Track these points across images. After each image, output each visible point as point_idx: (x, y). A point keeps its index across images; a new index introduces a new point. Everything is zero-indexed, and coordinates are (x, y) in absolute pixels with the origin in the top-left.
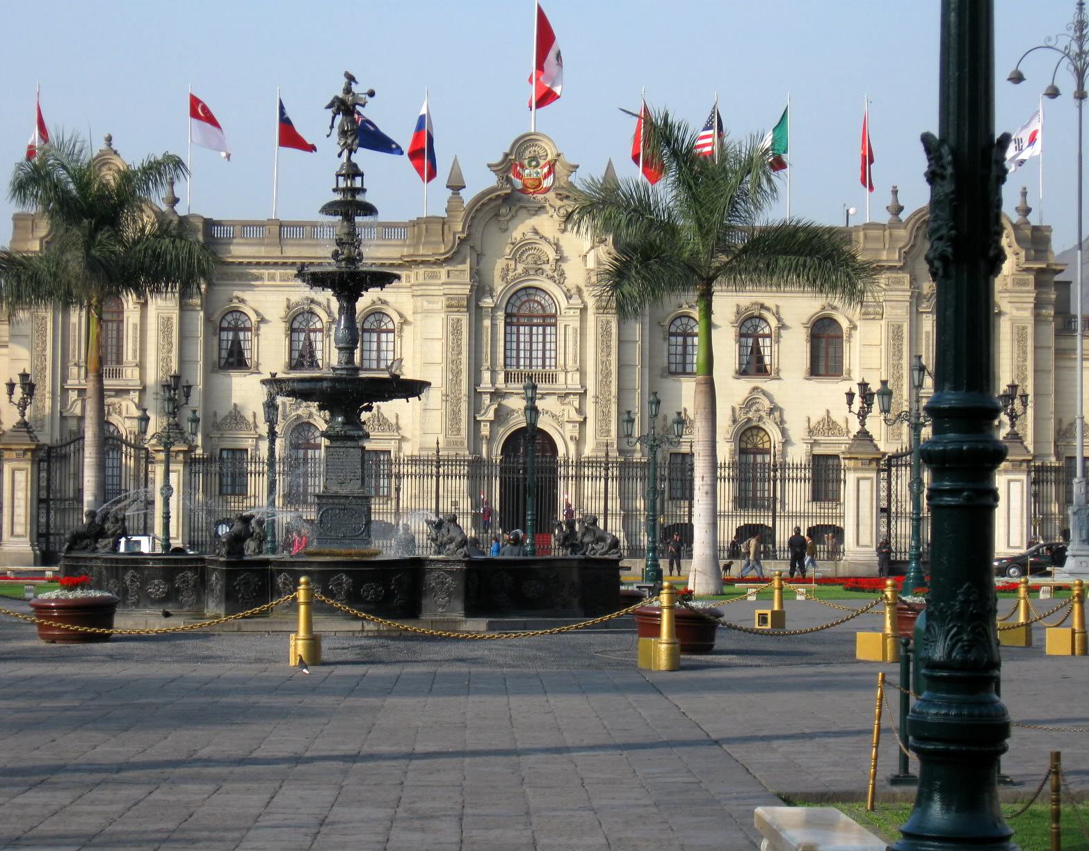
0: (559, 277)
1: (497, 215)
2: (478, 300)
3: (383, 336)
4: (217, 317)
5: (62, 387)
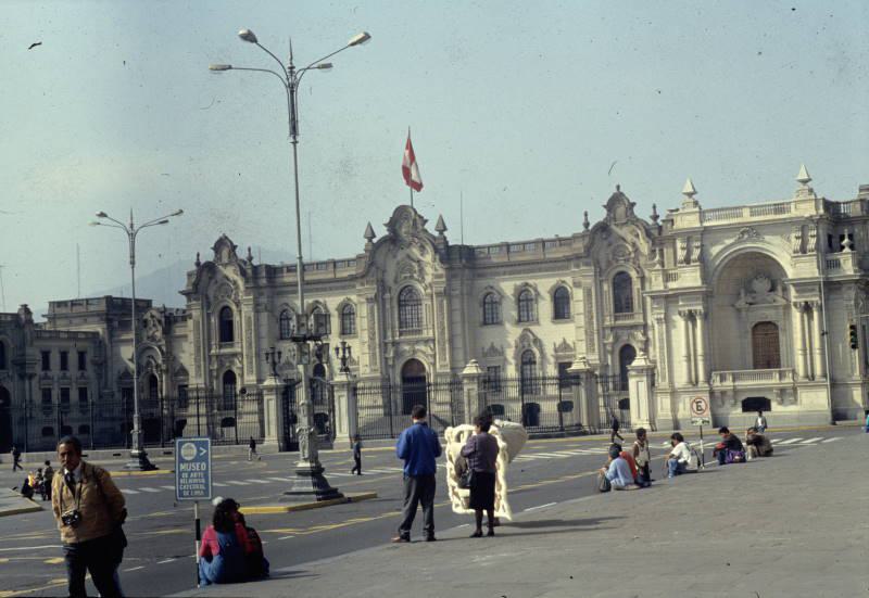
0: (423, 278)
2: (384, 294)
4: (278, 314)
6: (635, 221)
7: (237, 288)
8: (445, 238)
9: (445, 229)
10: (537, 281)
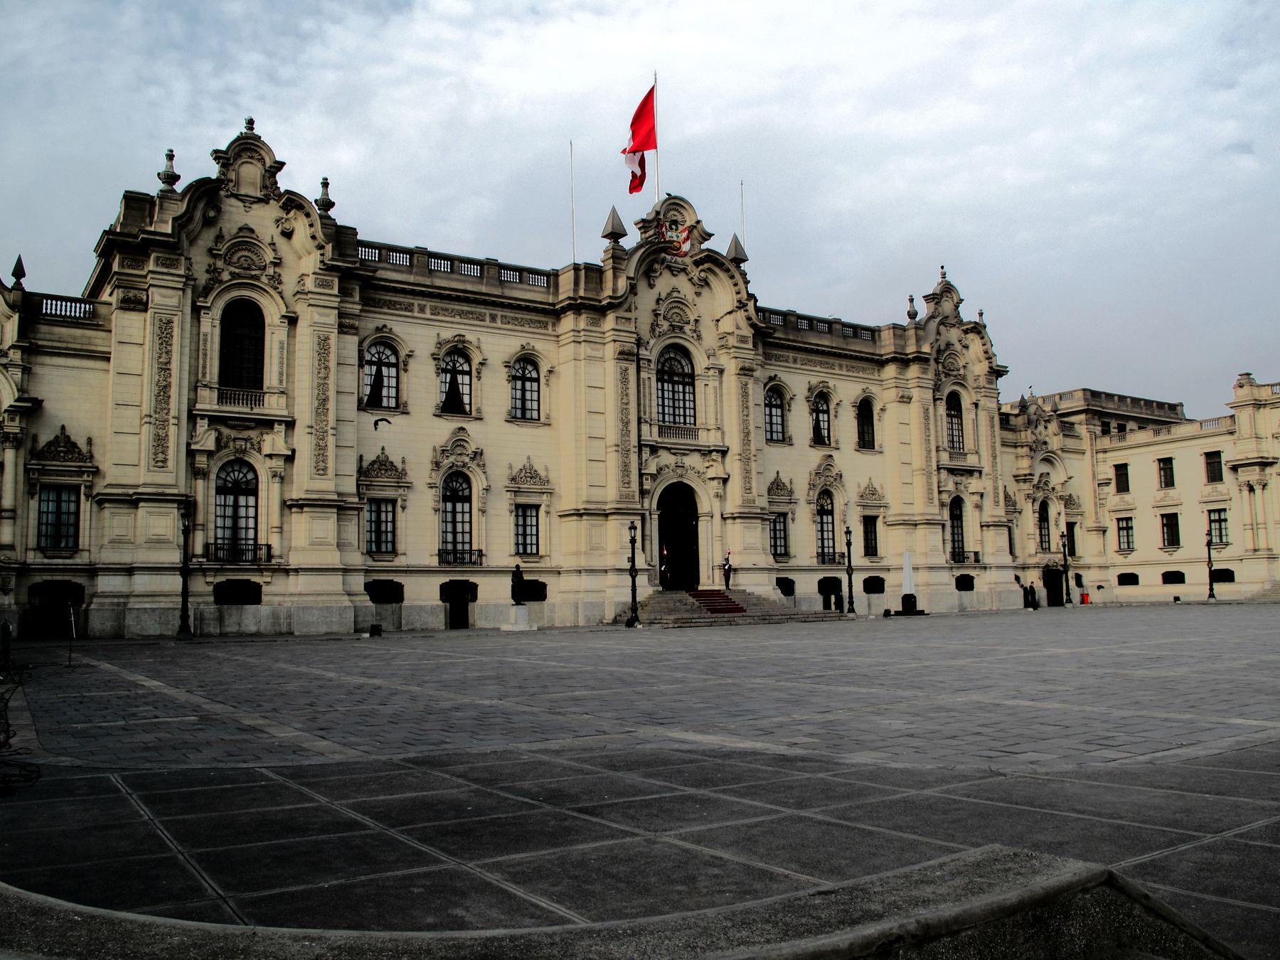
0: (699, 338)
3: (528, 385)
5: (190, 411)
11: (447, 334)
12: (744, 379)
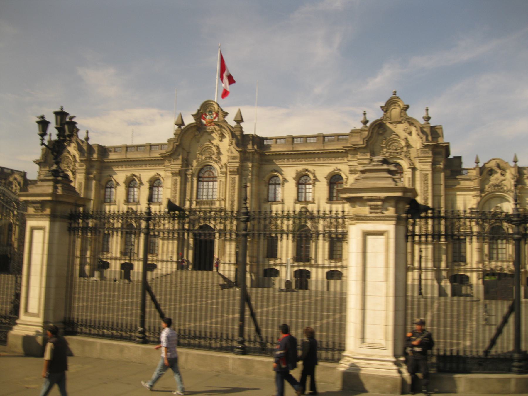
0: (220, 159)
1: (195, 136)
4: (103, 182)
6: (411, 122)
7: (75, 161)
8: (241, 128)
9: (242, 121)
10: (315, 168)
11: (129, 174)
12: (233, 176)
